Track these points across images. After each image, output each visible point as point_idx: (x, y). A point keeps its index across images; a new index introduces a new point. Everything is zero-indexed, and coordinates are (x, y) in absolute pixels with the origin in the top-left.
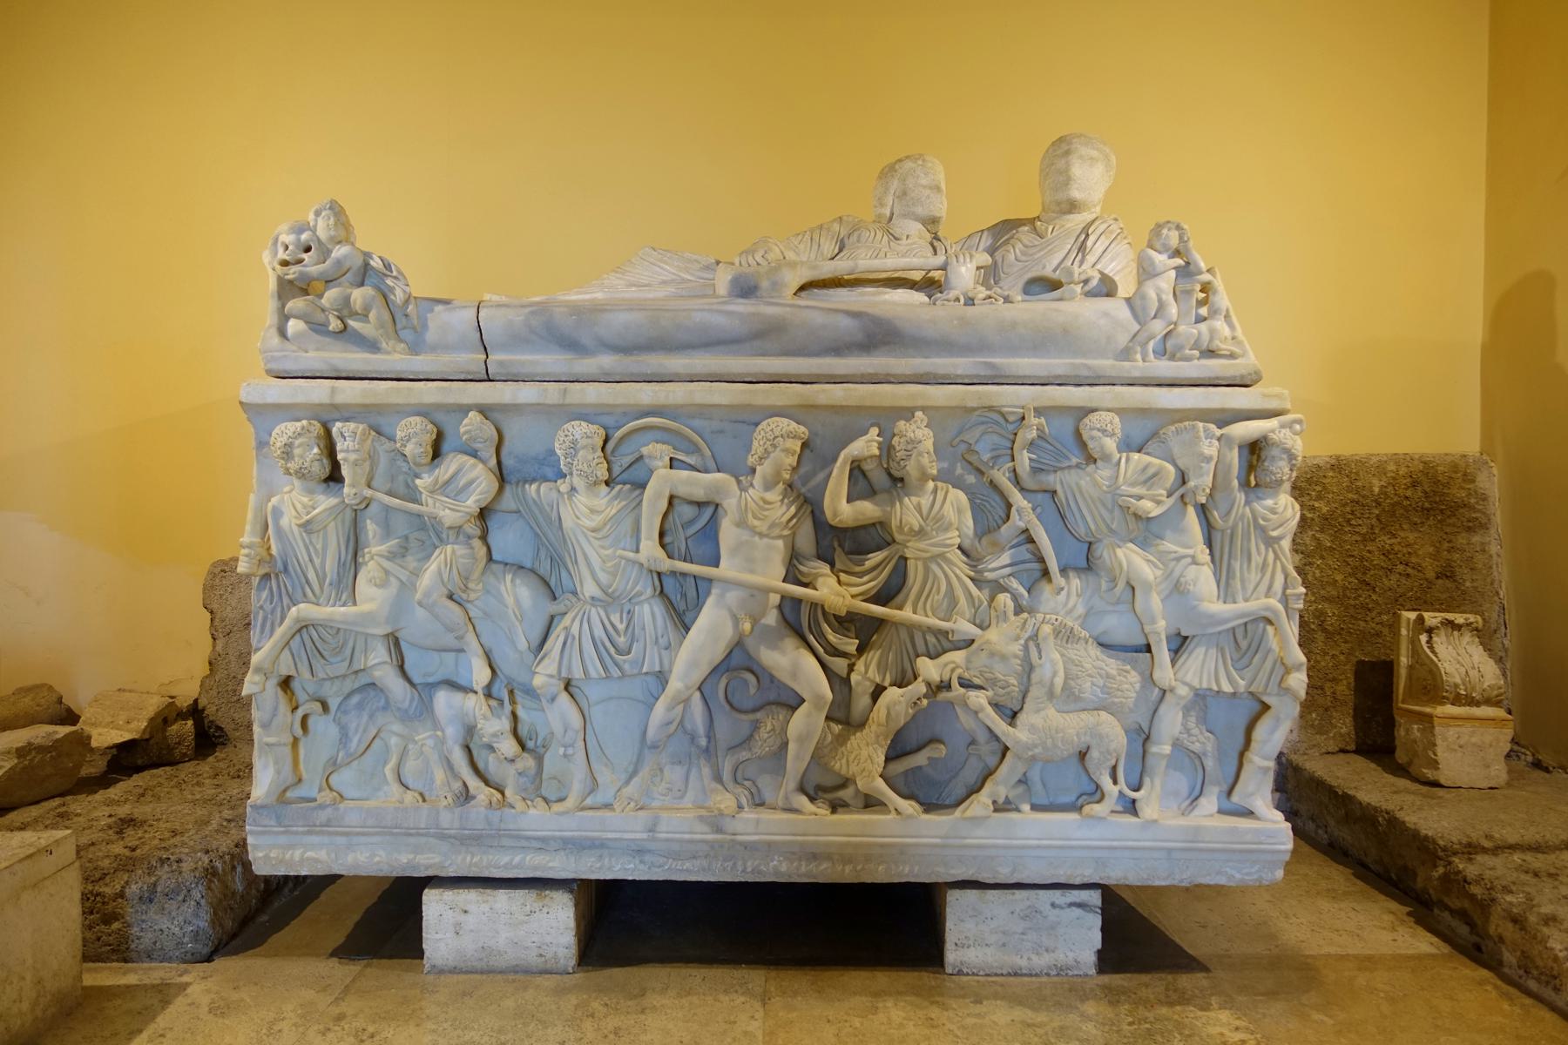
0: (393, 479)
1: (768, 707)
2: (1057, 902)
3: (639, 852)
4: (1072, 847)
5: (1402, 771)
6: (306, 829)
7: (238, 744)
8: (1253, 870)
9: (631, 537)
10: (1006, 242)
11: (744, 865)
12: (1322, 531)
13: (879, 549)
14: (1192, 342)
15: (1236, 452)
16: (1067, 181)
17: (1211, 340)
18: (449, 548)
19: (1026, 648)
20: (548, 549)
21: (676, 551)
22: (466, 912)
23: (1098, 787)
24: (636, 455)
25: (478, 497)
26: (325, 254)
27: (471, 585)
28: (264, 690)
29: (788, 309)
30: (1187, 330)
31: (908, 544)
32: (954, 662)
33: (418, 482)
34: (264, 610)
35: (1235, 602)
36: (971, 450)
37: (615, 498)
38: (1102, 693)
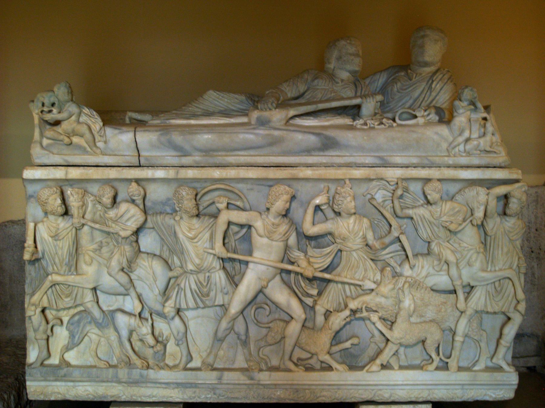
0: (95, 214)
1: (274, 322)
4: (417, 385)
8: (500, 393)
19: (398, 293)
21: (230, 246)
23: (431, 357)
24: (211, 201)
36: (373, 198)
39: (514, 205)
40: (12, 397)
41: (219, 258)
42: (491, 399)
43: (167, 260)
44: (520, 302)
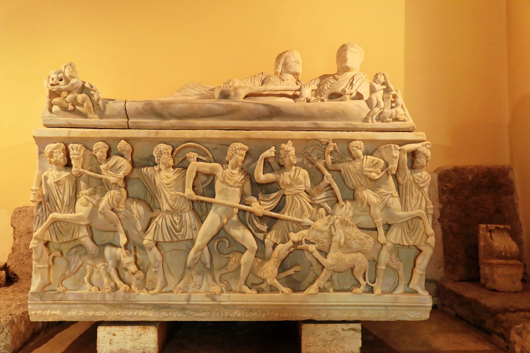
2: (344, 328)
3: (183, 309)
5: (484, 286)
6: (52, 302)
7: (23, 281)
9: (182, 187)
10: (324, 83)
11: (224, 314)
12: (450, 195)
13: (275, 192)
14: (389, 116)
15: (406, 155)
16: (345, 60)
17: (396, 115)
18: (112, 191)
19: (330, 228)
20: (150, 193)
22: (114, 335)
23: (359, 282)
24: (184, 157)
25: (124, 172)
26: (68, 82)
27: (121, 206)
28: (38, 246)
29: (241, 103)
30: (388, 111)
31: (286, 190)
32: (303, 234)
33: (101, 166)
34: (39, 216)
35: (408, 211)
37: (176, 173)
38: (359, 245)
39: (421, 160)
40: (23, 322)
41: (189, 200)
42: (410, 320)
43: (150, 204)
44: (430, 237)
